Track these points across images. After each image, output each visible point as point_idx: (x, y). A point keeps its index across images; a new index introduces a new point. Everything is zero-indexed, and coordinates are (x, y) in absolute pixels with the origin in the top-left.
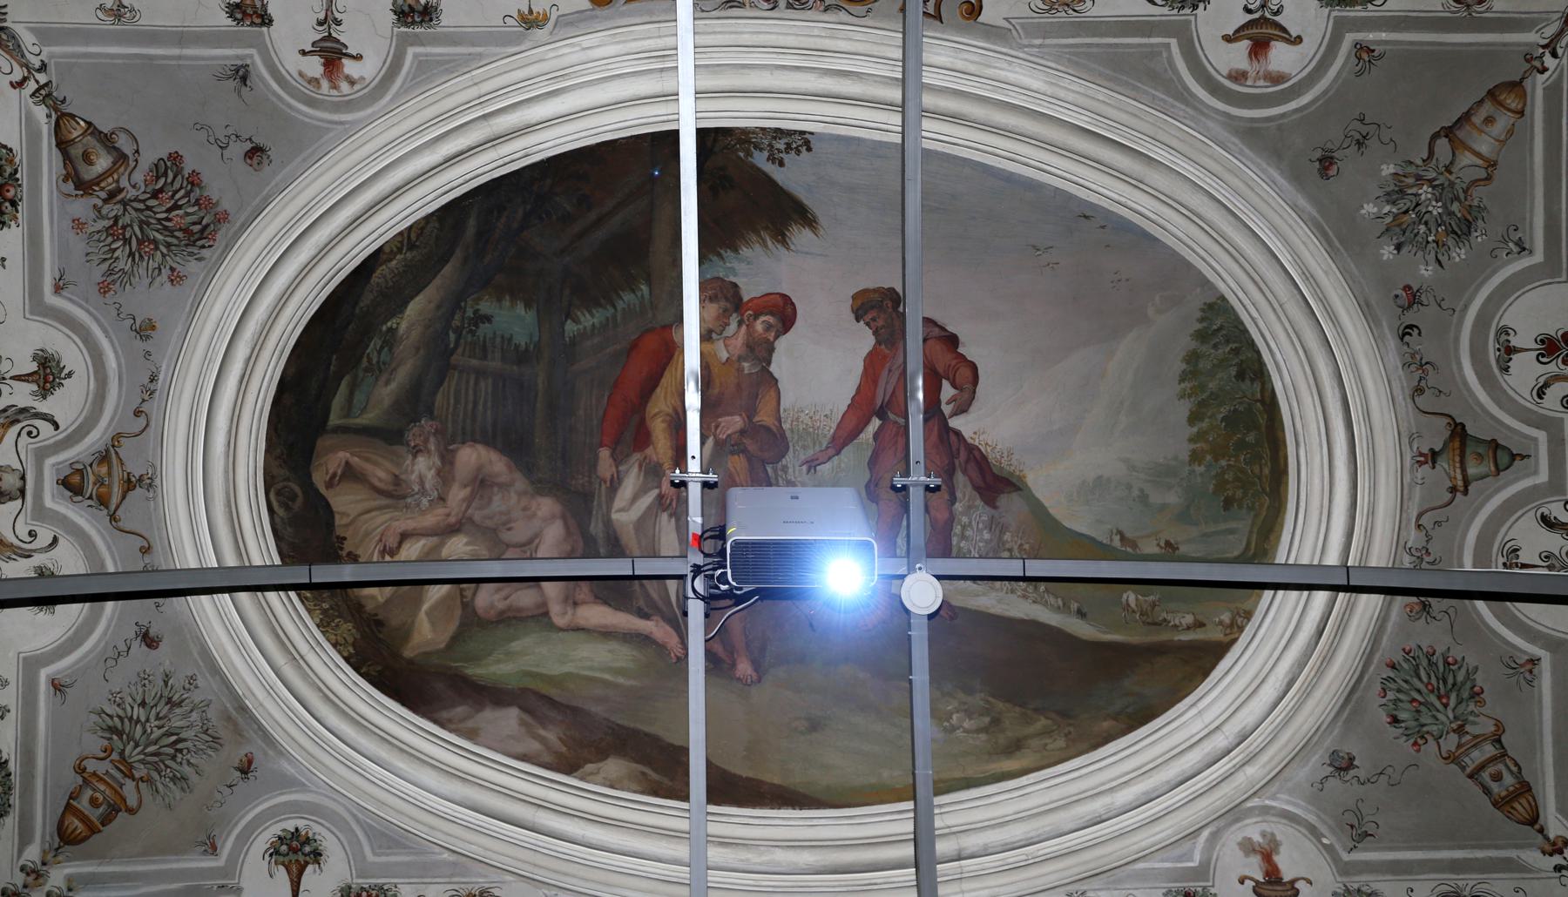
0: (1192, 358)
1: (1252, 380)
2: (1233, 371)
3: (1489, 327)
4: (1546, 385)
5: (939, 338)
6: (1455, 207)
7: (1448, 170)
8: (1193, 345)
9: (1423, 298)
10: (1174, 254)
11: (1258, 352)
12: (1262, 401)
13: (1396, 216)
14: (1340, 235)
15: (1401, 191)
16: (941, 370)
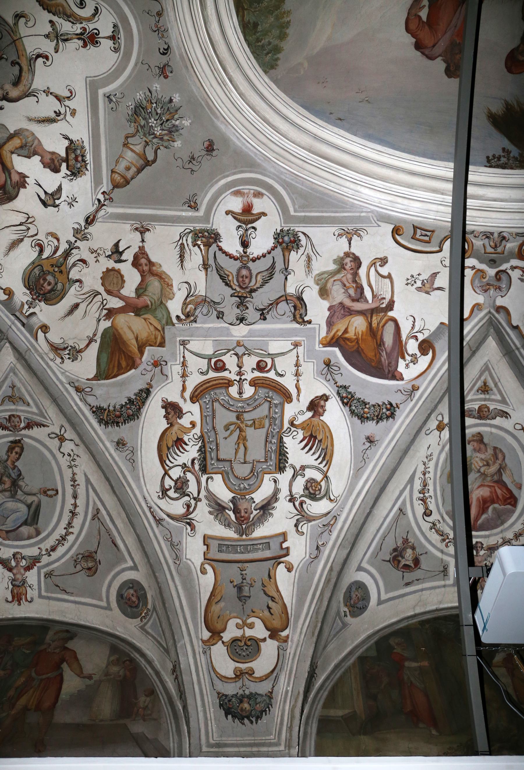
0: (283, 36)
1: (249, 22)
2: (260, 28)
3: (124, 53)
4: (94, 15)
5: (426, 47)
6: (143, 122)
7: (147, 143)
8: (283, 44)
9: (158, 71)
10: (292, 98)
11: (246, 40)
12: (243, 9)
13: (173, 118)
14: (202, 109)
15: (170, 132)
16: (427, 27)
